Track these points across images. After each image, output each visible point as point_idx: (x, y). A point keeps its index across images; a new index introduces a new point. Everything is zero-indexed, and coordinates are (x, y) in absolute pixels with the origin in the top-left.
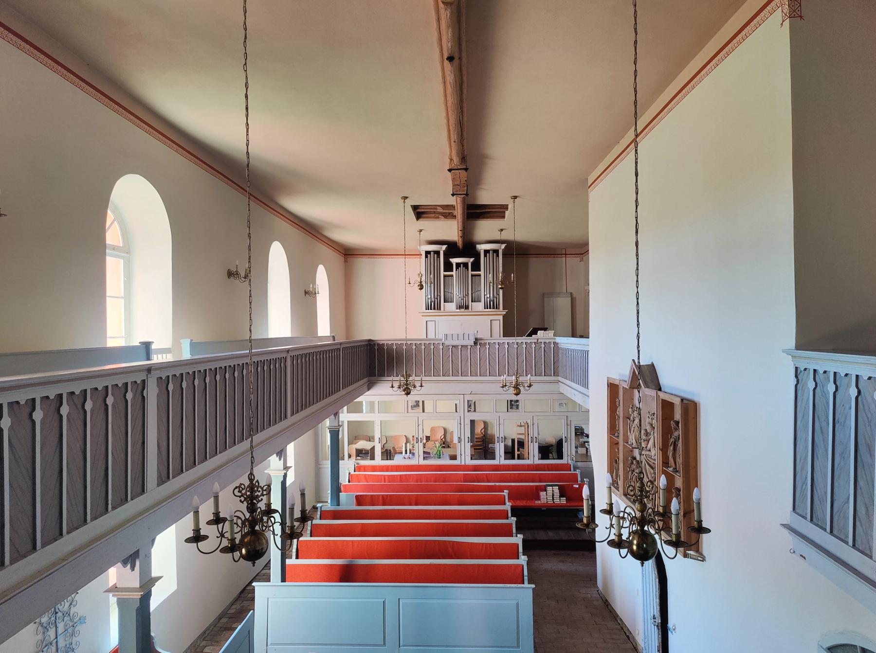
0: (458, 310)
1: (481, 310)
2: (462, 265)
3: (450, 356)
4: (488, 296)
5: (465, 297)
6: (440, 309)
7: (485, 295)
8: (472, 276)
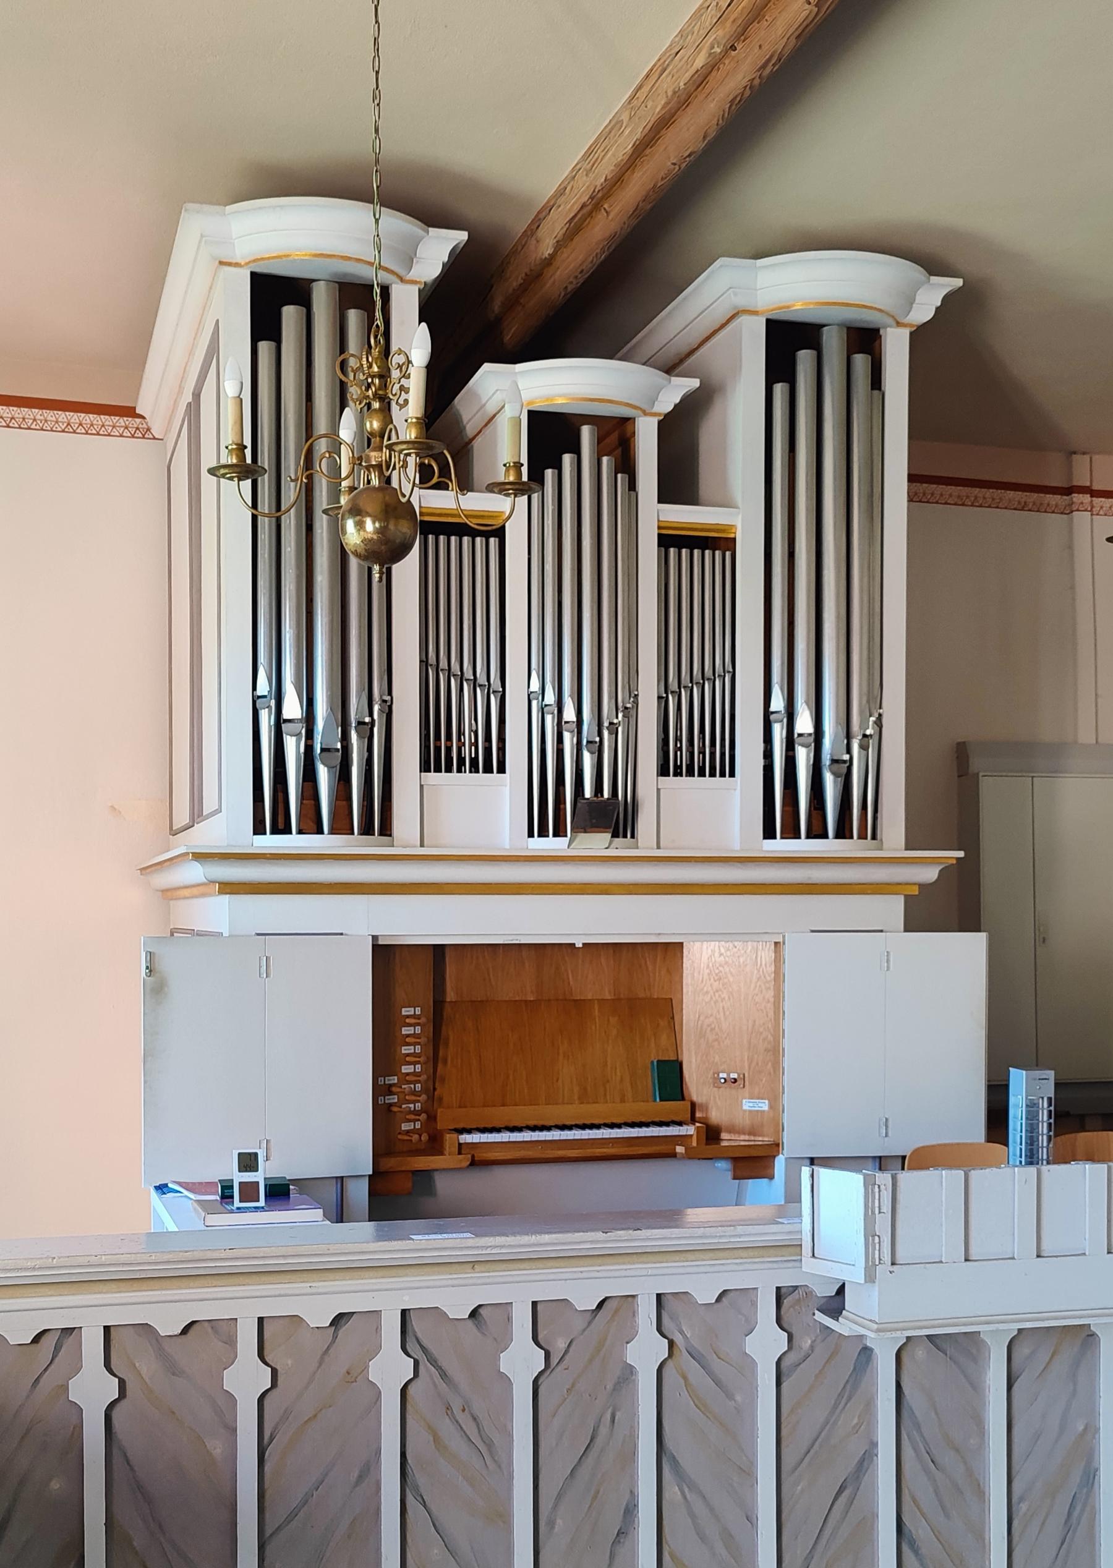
0: (552, 844)
1: (735, 845)
2: (586, 431)
3: (868, 1458)
4: (804, 724)
5: (613, 729)
6: (386, 830)
7: (767, 714)
8: (668, 540)
